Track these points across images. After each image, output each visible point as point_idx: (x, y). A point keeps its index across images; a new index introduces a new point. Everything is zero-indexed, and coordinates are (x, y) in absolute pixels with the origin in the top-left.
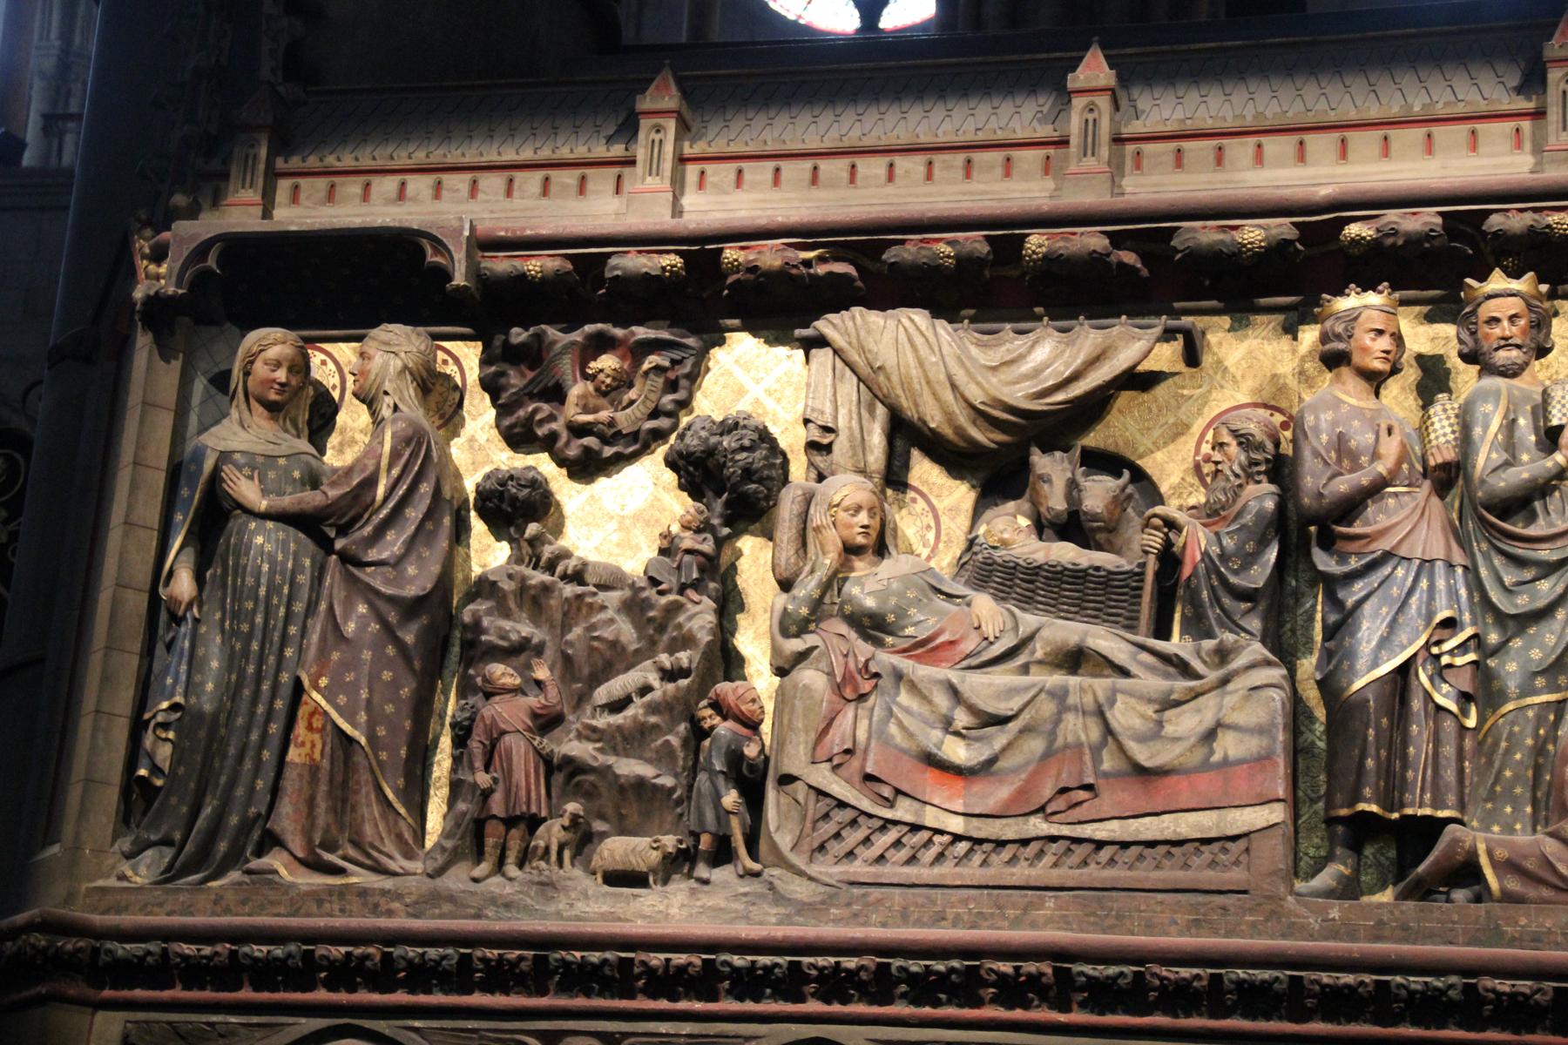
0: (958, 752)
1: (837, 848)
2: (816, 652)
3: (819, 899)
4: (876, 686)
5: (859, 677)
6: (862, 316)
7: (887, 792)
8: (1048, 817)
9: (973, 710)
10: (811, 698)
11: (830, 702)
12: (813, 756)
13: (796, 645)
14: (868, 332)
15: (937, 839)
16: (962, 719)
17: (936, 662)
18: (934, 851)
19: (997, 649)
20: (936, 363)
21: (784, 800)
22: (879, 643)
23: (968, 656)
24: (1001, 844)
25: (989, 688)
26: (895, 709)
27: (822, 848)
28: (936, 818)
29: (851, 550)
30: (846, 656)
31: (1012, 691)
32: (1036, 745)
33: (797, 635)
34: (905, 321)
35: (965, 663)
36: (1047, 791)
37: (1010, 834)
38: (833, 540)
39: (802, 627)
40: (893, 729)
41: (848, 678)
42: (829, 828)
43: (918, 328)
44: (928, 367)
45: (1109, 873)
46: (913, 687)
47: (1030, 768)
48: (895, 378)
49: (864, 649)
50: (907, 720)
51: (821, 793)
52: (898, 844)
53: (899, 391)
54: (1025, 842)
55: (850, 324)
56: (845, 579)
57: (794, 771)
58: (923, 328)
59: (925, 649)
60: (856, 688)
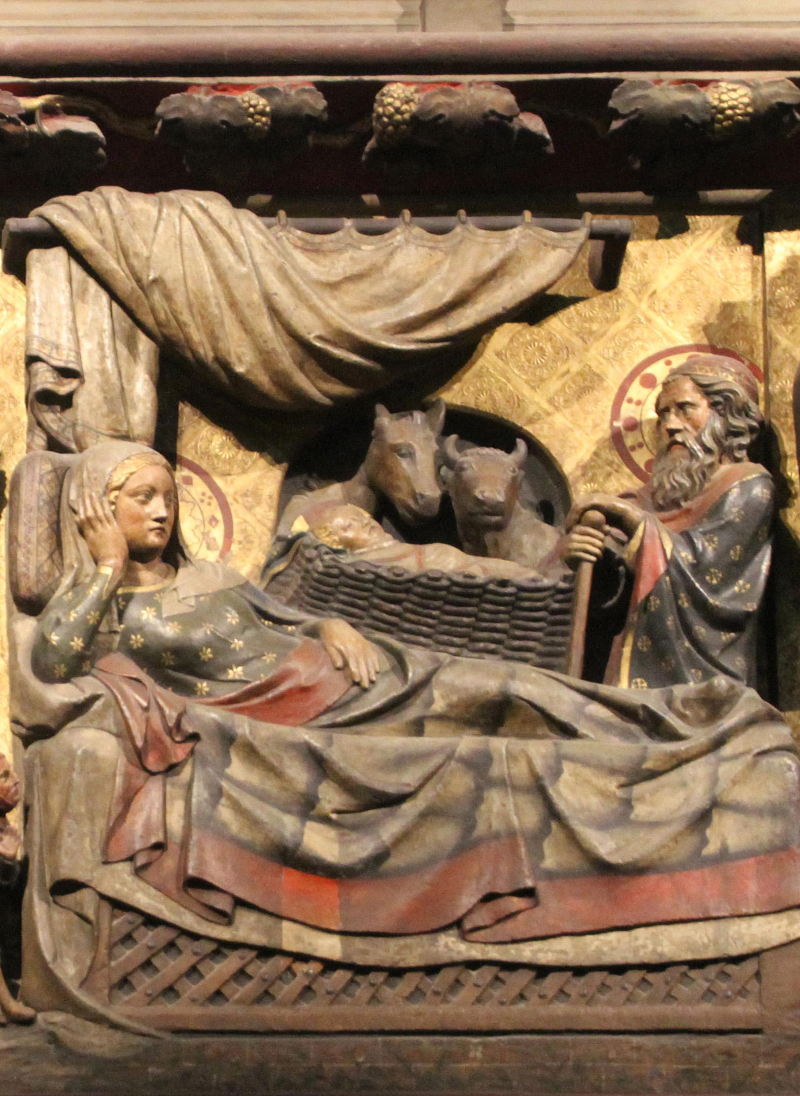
0: (321, 843)
1: (145, 983)
2: (98, 704)
3: (130, 1053)
4: (192, 752)
5: (167, 740)
6: (121, 199)
7: (222, 903)
8: (464, 936)
9: (347, 785)
10: (97, 770)
11: (127, 776)
12: (105, 851)
13: (61, 695)
14: (134, 225)
15: (301, 968)
16: (330, 798)
17: (281, 719)
18: (299, 982)
19: (374, 701)
20: (247, 276)
21: (59, 916)
22: (188, 690)
23: (329, 709)
24: (396, 973)
25: (366, 753)
26: (224, 784)
27: (125, 983)
28: (299, 939)
29: (138, 554)
30: (146, 709)
31: (402, 761)
32: (445, 834)
33: (65, 679)
34: (192, 210)
35: (325, 720)
36: (467, 900)
37: (413, 959)
38: (112, 539)
39: (77, 666)
40: (225, 813)
41: (152, 741)
42: (129, 955)
43: (214, 222)
44: (233, 282)
45: (560, 1008)
46: (251, 753)
47: (438, 867)
48: (180, 298)
49: (169, 702)
50: (248, 802)
51: (118, 905)
52: (241, 975)
53: (186, 317)
54: (432, 970)
55: (103, 213)
56: (128, 598)
57: (81, 875)
58: (224, 223)
59: (268, 699)
60: (164, 754)
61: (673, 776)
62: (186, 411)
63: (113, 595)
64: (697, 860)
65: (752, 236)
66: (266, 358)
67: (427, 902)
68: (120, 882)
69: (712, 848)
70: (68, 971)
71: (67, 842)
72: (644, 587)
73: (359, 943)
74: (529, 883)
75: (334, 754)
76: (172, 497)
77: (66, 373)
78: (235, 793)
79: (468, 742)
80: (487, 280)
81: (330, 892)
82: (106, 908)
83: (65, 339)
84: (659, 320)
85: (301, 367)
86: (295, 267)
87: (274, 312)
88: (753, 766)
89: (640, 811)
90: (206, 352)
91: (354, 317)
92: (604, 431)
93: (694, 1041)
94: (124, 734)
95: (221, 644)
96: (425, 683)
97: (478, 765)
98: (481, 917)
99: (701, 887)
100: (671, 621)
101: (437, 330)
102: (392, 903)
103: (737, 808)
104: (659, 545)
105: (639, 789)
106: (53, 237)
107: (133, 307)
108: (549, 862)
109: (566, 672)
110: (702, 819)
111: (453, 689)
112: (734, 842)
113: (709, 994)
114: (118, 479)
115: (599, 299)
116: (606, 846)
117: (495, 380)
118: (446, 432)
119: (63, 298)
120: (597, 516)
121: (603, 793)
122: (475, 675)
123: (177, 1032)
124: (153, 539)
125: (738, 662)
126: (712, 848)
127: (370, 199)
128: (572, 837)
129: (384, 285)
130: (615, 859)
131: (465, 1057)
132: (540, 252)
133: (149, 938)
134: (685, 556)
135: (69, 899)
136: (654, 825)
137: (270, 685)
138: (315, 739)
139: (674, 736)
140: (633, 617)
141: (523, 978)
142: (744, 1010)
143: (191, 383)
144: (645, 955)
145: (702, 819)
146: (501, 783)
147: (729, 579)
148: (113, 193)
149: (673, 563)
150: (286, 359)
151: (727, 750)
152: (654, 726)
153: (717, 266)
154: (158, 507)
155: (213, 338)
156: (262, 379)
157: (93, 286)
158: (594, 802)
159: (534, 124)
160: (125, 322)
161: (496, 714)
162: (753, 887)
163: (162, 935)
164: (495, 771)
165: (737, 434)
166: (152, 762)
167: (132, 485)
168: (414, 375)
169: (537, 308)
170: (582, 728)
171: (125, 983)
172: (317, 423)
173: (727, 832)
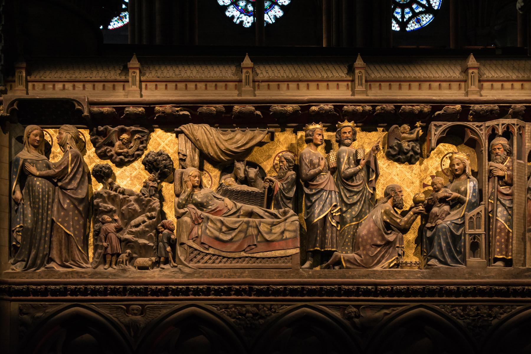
1: (195, 260)
7: (207, 247)
9: (227, 227)
13: (182, 211)
16: (224, 229)
19: (232, 212)
21: (182, 249)
22: (202, 210)
24: (234, 258)
25: (230, 221)
29: (194, 187)
31: (236, 222)
32: (242, 235)
33: (182, 208)
36: (245, 246)
37: (237, 256)
38: (190, 184)
40: (207, 231)
45: (260, 264)
48: (202, 143)
49: (199, 212)
52: (210, 259)
53: (203, 146)
54: (240, 258)
56: (193, 194)
57: (184, 242)
59: (215, 212)
60: (198, 221)
61: (278, 225)
62: (205, 161)
63: (190, 193)
64: (282, 240)
65: (295, 132)
66: (216, 153)
68: (191, 243)
69: (284, 238)
70: (182, 258)
71: (182, 236)
72: (275, 193)
74: (256, 243)
75: (225, 221)
76: (200, 177)
77: (184, 155)
78: (209, 228)
79: (246, 219)
82: (189, 248)
83: (184, 150)
84: (281, 146)
85: (222, 154)
87: (217, 145)
88: (291, 224)
89: (273, 231)
90: (206, 152)
92: (272, 165)
93: (281, 270)
94: (191, 218)
97: (248, 223)
99: (283, 244)
100: (280, 198)
101: (243, 148)
102: (234, 247)
103: (288, 231)
104: (278, 185)
105: (273, 227)
106: (182, 132)
107: (195, 144)
108: (259, 240)
110: (283, 233)
111: (244, 210)
112: (288, 237)
113: (284, 262)
114: (191, 174)
115: (271, 142)
116: (267, 237)
117: (255, 156)
118: (246, 165)
119: (184, 142)
121: (267, 228)
123: (200, 268)
125: (290, 205)
126: (284, 238)
127: (234, 125)
129: (235, 140)
130: (269, 239)
132: (260, 135)
133: (195, 252)
135: (182, 246)
138: (222, 218)
139: (279, 218)
140: (274, 198)
142: (289, 264)
143: (204, 157)
144: (273, 256)
145: (283, 233)
146: (251, 226)
147: (289, 192)
149: (280, 188)
151: (287, 221)
152: (276, 217)
153: (290, 137)
154: (197, 179)
155: (207, 150)
156: (215, 157)
157: (189, 140)
158: (266, 229)
160: (194, 146)
162: (291, 244)
163: (198, 252)
164: (250, 224)
165: (291, 166)
167: (193, 175)
168: (241, 155)
169: (261, 144)
171: (191, 260)
173: (287, 235)
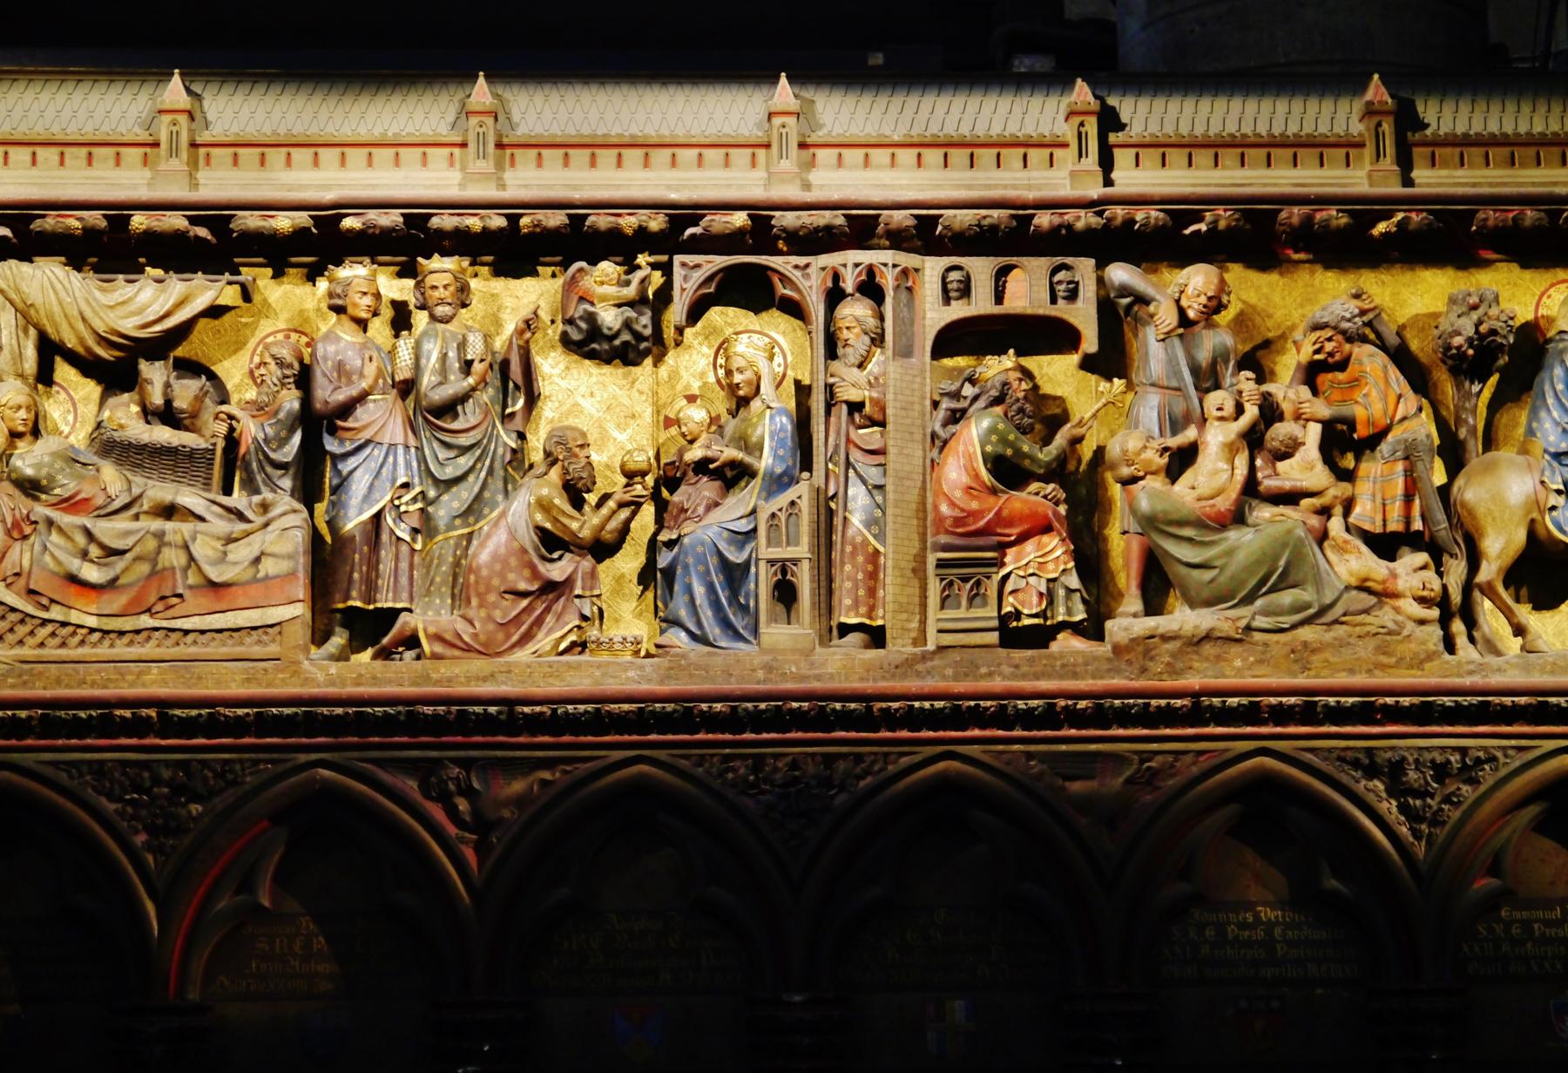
0: (92, 574)
7: (45, 601)
9: (102, 546)
16: (94, 551)
18: (78, 639)
19: (117, 504)
22: (37, 499)
24: (121, 633)
25: (110, 530)
29: (15, 435)
32: (144, 569)
36: (153, 599)
37: (128, 628)
41: (16, 525)
46: (60, 530)
48: (42, 313)
49: (24, 505)
50: (57, 553)
53: (45, 321)
54: (138, 632)
59: (71, 504)
60: (21, 531)
66: (82, 341)
67: (136, 600)
72: (242, 450)
73: (105, 619)
75: (96, 532)
79: (157, 524)
80: (180, 304)
81: (93, 595)
86: (95, 299)
87: (84, 319)
88: (280, 536)
89: (231, 557)
91: (120, 322)
95: (51, 478)
96: (140, 496)
97: (160, 536)
98: (159, 607)
99: (255, 592)
100: (254, 465)
101: (158, 328)
104: (251, 430)
108: (191, 581)
109: (209, 490)
110: (257, 560)
111: (151, 500)
112: (271, 572)
113: (259, 642)
116: (215, 574)
120: (223, 416)
121: (214, 548)
122: (162, 491)
124: (21, 429)
126: (261, 575)
128: (199, 569)
129: (132, 307)
130: (216, 580)
131: (149, 673)
134: (261, 436)
136: (235, 563)
137: (71, 497)
138: (88, 522)
139: (249, 521)
141: (175, 636)
142: (273, 649)
145: (257, 560)
146: (169, 544)
148: (13, 263)
149: (255, 439)
150: (91, 342)
151: (270, 528)
152: (241, 516)
154: (22, 414)
156: (80, 350)
158: (210, 553)
159: (203, 232)
161: (169, 511)
164: (167, 539)
166: (16, 535)
170: (207, 517)
172: (115, 369)
173: (269, 567)
